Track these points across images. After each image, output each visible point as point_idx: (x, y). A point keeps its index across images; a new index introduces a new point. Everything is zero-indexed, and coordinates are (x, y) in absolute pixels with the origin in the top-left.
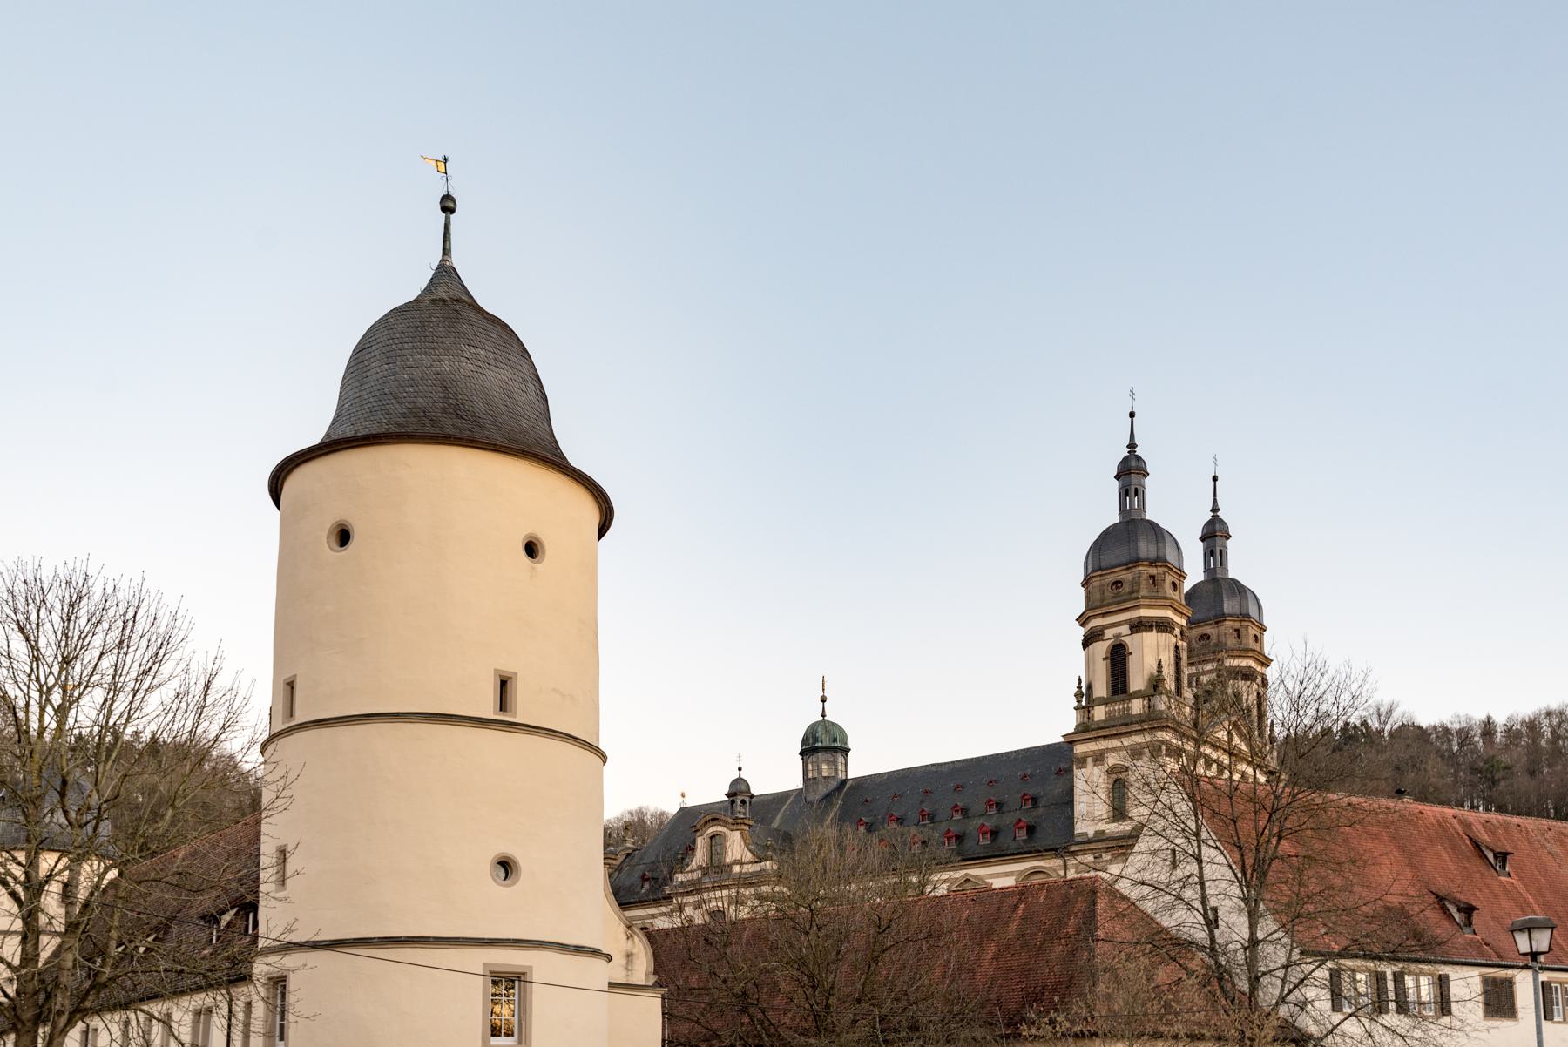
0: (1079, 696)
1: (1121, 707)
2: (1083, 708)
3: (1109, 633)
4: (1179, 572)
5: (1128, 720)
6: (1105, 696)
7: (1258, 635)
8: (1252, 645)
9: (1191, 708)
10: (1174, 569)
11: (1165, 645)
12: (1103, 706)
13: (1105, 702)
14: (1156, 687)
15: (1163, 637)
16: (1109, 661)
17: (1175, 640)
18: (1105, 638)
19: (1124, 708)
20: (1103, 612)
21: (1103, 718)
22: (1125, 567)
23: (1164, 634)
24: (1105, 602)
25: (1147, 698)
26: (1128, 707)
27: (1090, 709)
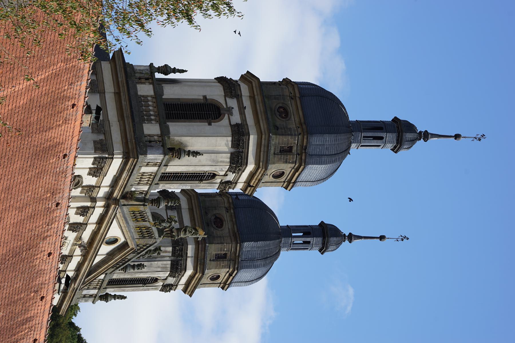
0: (166, 69)
1: (152, 113)
2: (153, 75)
3: (233, 103)
4: (293, 181)
5: (137, 119)
6: (164, 97)
7: (219, 281)
8: (209, 273)
9: (147, 192)
10: (297, 174)
11: (218, 162)
12: (152, 93)
13: (158, 94)
14: (172, 150)
15: (226, 158)
16: (202, 101)
17: (223, 173)
18: (227, 99)
19: (151, 115)
20: (256, 97)
22: (302, 121)
23: (228, 160)
24: (266, 100)
25: (160, 139)
26: (152, 120)
27: (150, 81)
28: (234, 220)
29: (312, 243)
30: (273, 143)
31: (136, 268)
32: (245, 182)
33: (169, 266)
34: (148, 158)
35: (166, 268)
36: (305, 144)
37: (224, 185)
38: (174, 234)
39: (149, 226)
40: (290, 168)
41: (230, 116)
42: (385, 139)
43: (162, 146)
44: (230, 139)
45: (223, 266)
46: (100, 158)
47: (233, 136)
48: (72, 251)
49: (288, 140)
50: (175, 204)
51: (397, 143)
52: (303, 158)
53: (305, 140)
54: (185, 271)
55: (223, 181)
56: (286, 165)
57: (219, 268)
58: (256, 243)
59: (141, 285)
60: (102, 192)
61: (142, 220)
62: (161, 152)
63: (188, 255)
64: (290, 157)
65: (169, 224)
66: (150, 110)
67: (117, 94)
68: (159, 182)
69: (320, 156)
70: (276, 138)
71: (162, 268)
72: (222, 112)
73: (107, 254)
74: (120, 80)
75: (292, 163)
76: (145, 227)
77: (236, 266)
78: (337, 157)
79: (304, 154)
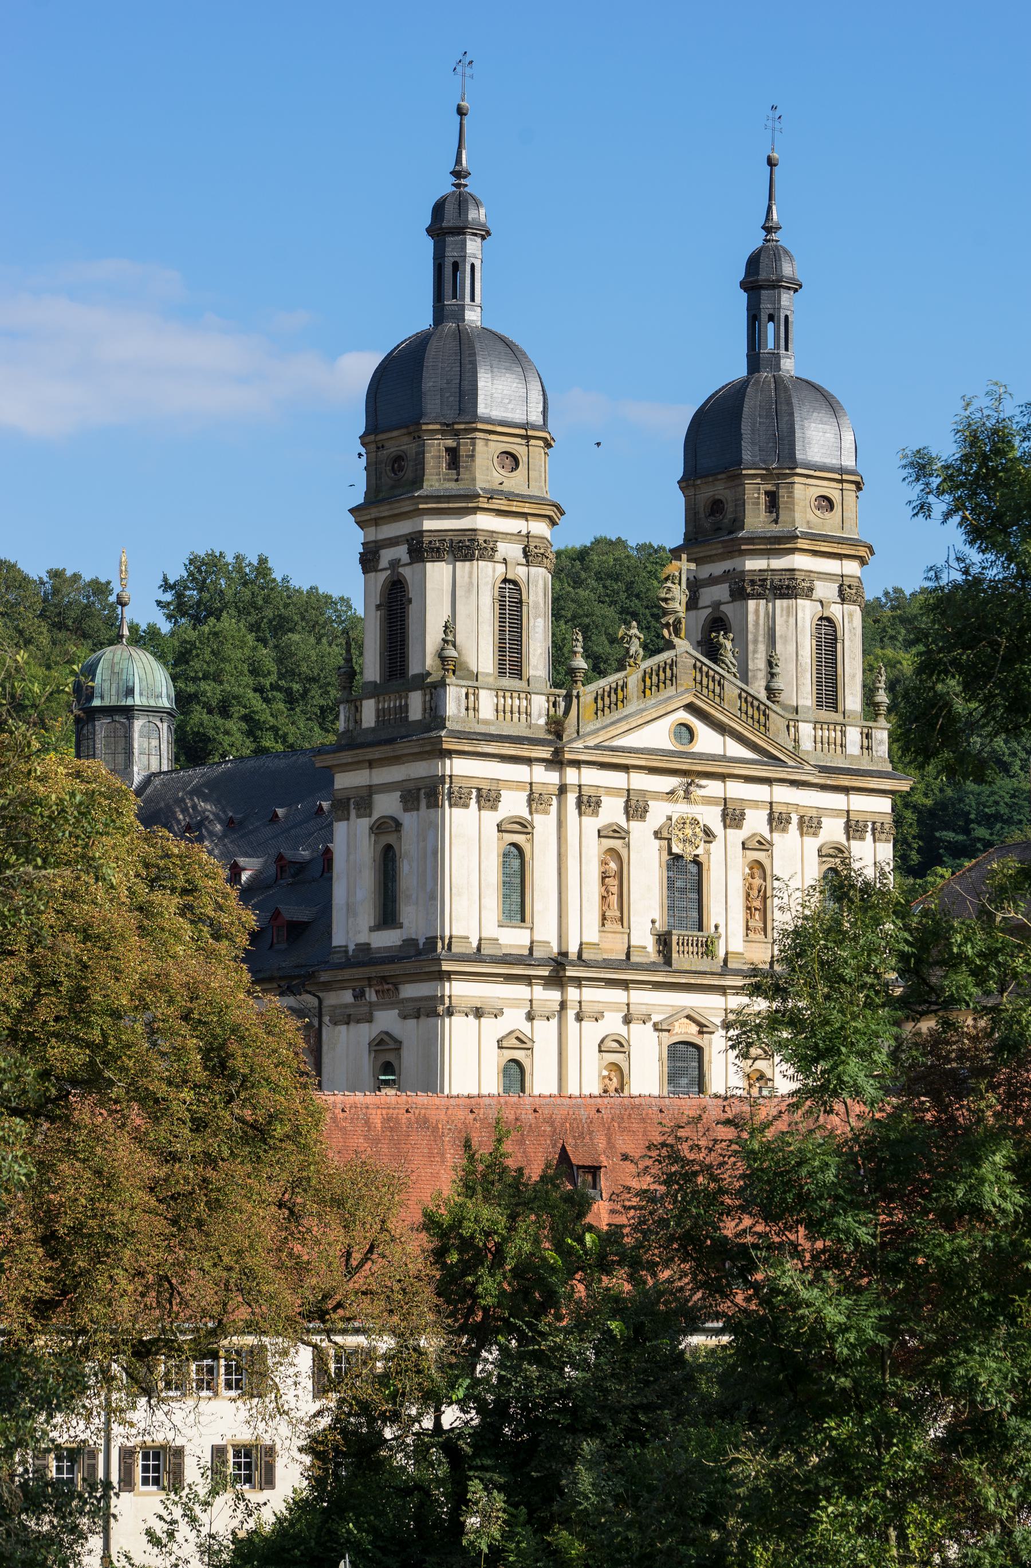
3: (387, 556)
17: (500, 568)
18: (380, 567)
20: (373, 516)
21: (373, 725)
23: (467, 563)
25: (428, 691)
28: (711, 479)
29: (771, 312)
30: (437, 484)
31: (774, 671)
32: (527, 520)
33: (785, 602)
34: (456, 712)
35: (788, 607)
36: (438, 427)
37: (531, 558)
38: (671, 621)
39: (640, 674)
40: (487, 445)
41: (402, 563)
42: (456, 259)
43: (435, 688)
44: (429, 565)
45: (788, 497)
46: (450, 799)
47: (423, 560)
48: (709, 801)
49: (433, 457)
50: (578, 640)
51: (464, 234)
52: (462, 426)
53: (431, 427)
54: (794, 570)
55: (524, 561)
56: (477, 455)
57: (793, 504)
58: (744, 436)
59: (839, 646)
60: (546, 777)
61: (622, 690)
62: (442, 691)
63: (765, 567)
64: (463, 452)
65: (633, 639)
66: (395, 706)
67: (371, 764)
68: (525, 678)
69: (461, 394)
70: (428, 480)
71: (788, 616)
72: (395, 579)
73: (723, 735)
74: (350, 760)
75: (474, 445)
76: (644, 681)
77: (787, 471)
78: (466, 360)
79: (456, 427)
